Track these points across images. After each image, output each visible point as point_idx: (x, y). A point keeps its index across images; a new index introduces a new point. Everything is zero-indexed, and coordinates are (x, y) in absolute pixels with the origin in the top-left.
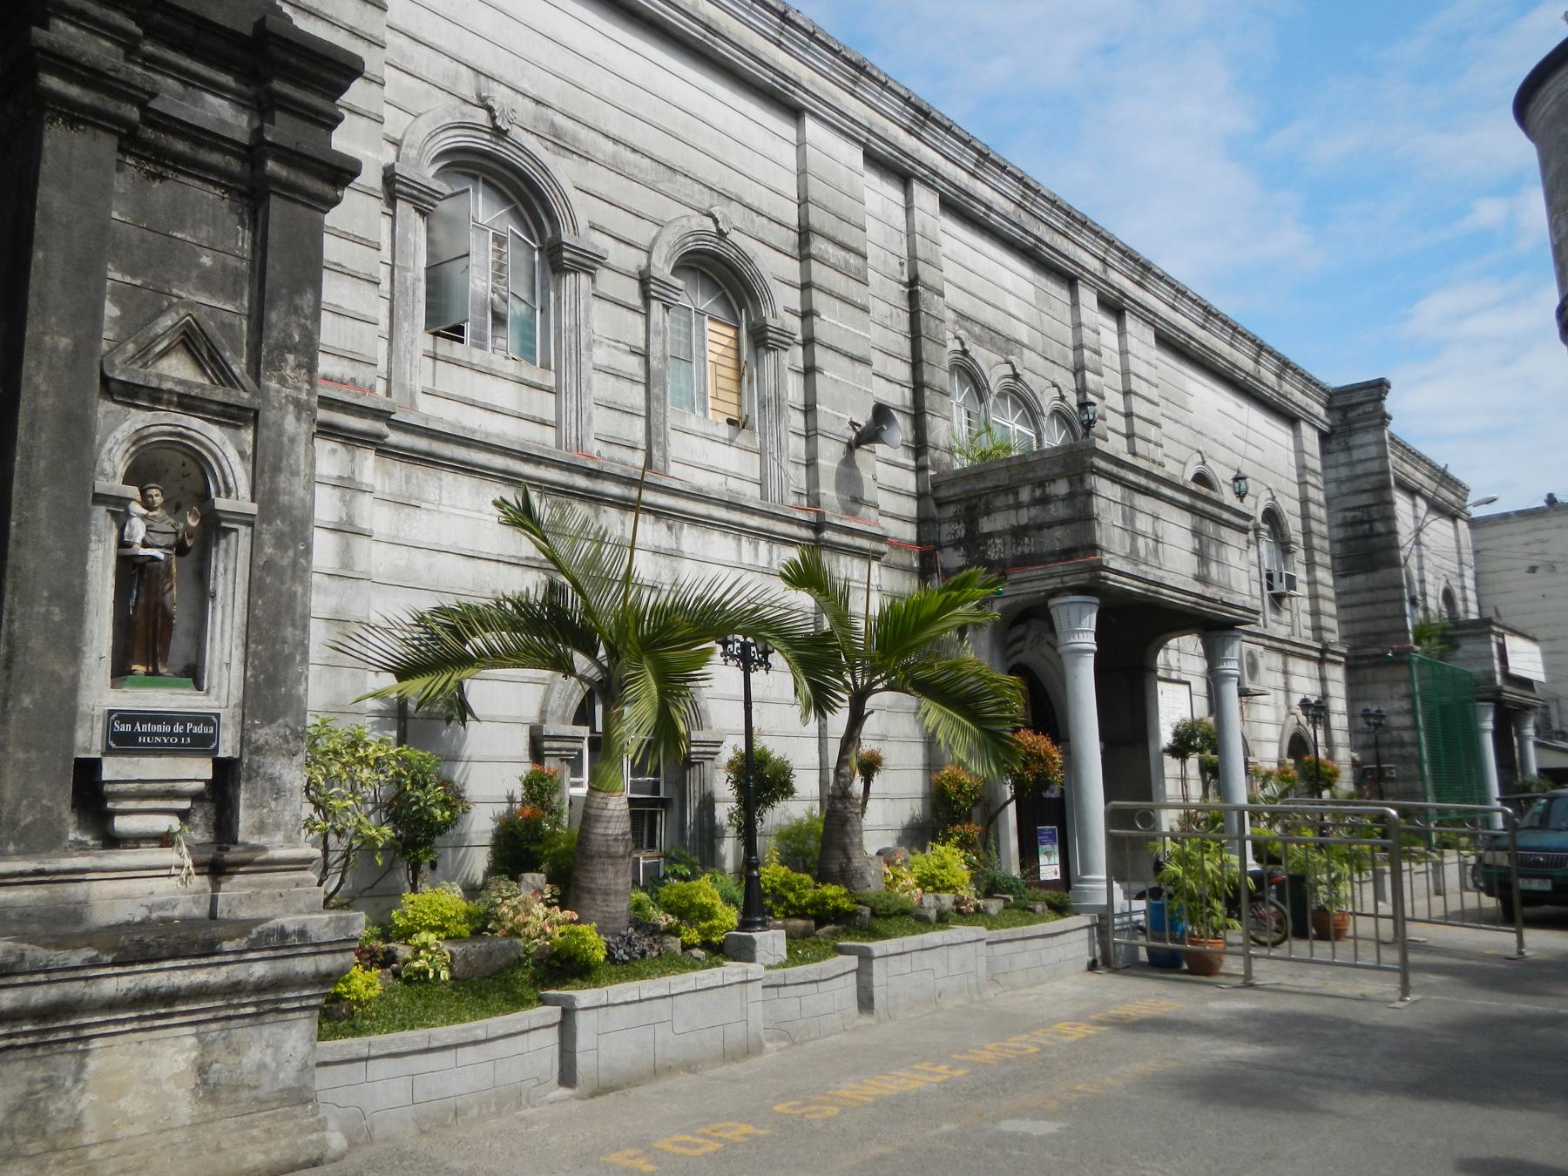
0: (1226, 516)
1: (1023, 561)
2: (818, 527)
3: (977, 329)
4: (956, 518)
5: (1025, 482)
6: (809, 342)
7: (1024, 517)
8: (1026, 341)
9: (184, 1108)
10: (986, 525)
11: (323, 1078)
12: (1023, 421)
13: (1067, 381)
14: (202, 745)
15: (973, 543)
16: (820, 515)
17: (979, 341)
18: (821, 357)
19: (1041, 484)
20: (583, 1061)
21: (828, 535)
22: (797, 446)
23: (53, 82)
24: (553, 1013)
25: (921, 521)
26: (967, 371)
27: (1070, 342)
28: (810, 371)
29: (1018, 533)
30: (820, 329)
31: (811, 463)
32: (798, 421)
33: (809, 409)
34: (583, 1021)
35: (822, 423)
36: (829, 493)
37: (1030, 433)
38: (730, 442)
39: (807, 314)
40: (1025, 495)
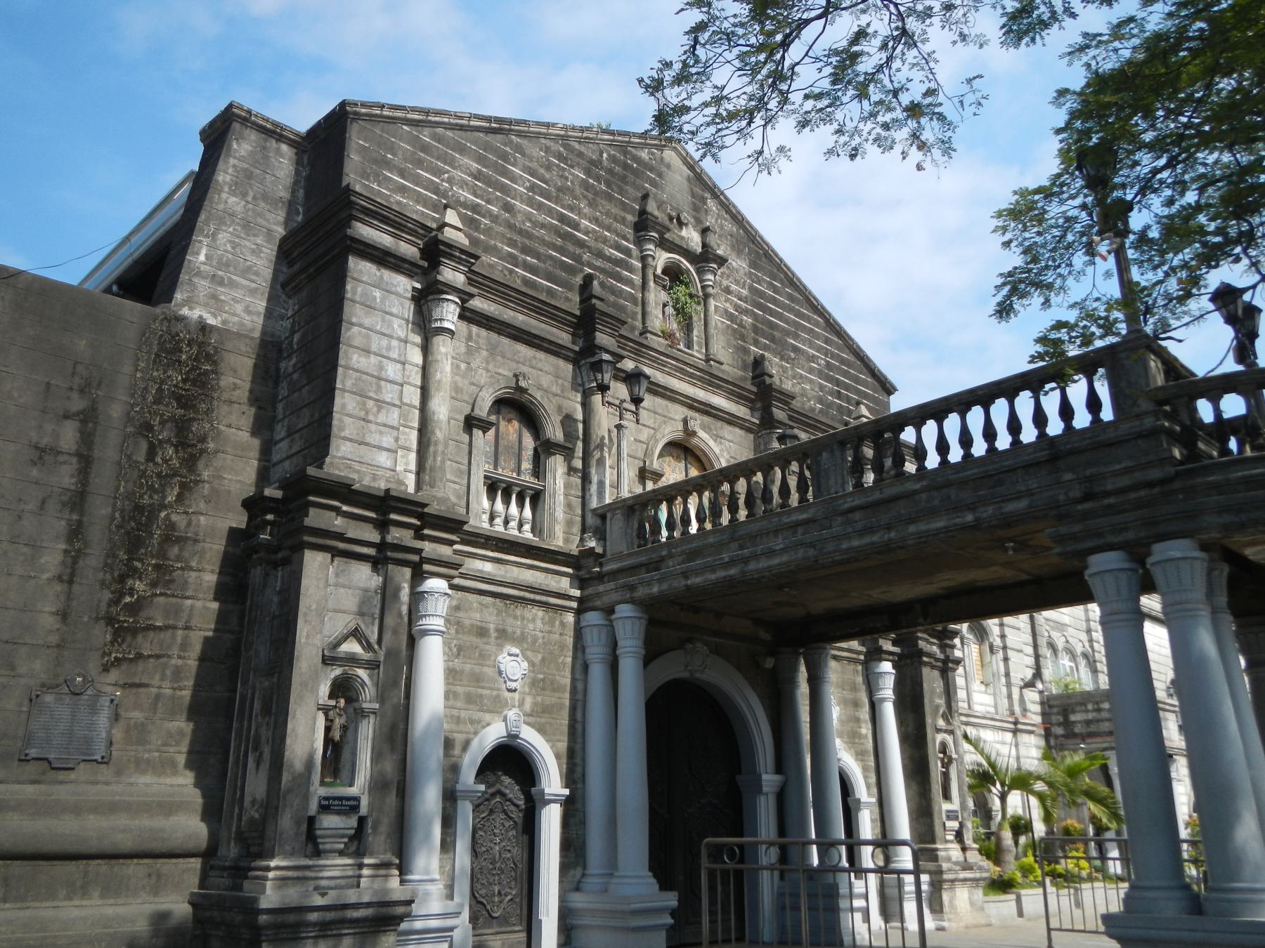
0: (1167, 707)
1: (1092, 735)
2: (1016, 723)
3: (1052, 624)
4: (1058, 713)
5: (1090, 701)
6: (1005, 648)
7: (1090, 716)
8: (1068, 623)
9: (968, 907)
10: (1073, 718)
11: (986, 905)
12: (1070, 660)
13: (1084, 637)
14: (956, 818)
15: (1067, 724)
16: (1016, 718)
17: (1053, 628)
18: (1010, 653)
19: (1097, 703)
20: (1025, 910)
21: (1020, 726)
22: (1004, 690)
23: (925, 659)
24: (1013, 897)
25: (1043, 714)
26: (1052, 646)
27: (1084, 618)
28: (1006, 659)
29: (1088, 723)
30: (1009, 643)
31: (1010, 696)
32: (1003, 680)
33: (1007, 675)
34: (1024, 899)
35: (1013, 681)
36: (1017, 709)
37: (1073, 664)
38: (986, 692)
39: (1003, 636)
40: (1090, 707)
